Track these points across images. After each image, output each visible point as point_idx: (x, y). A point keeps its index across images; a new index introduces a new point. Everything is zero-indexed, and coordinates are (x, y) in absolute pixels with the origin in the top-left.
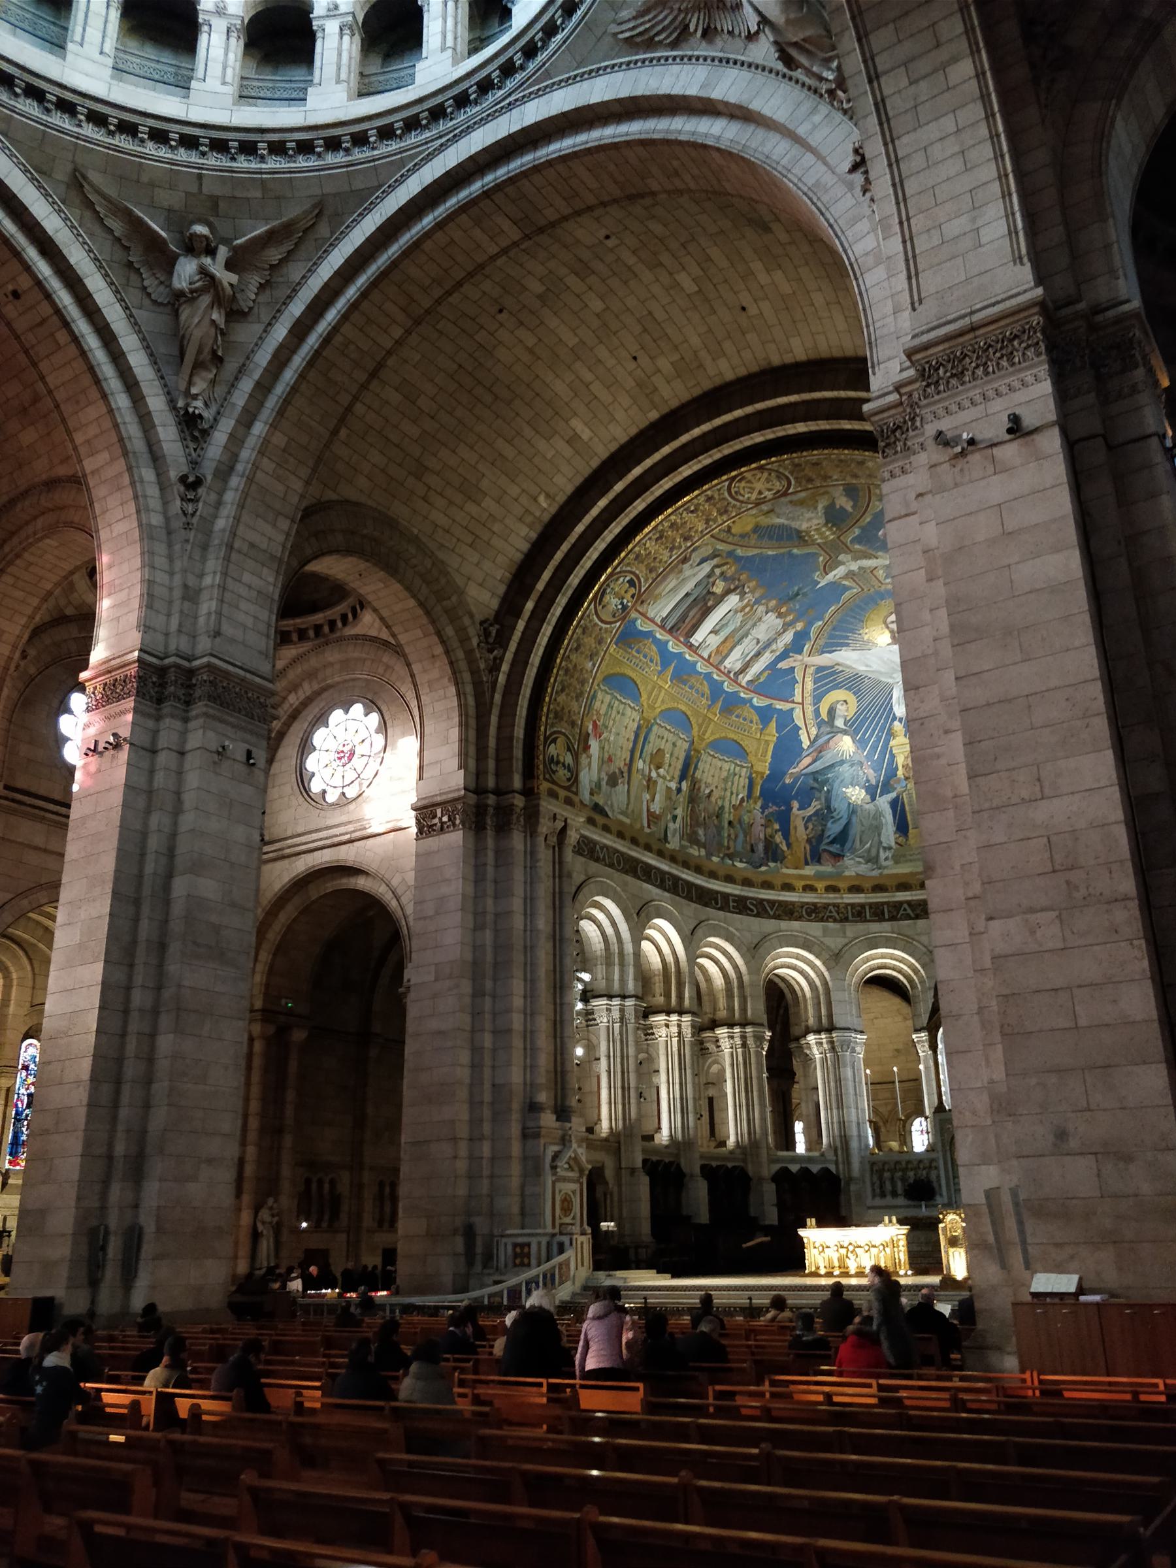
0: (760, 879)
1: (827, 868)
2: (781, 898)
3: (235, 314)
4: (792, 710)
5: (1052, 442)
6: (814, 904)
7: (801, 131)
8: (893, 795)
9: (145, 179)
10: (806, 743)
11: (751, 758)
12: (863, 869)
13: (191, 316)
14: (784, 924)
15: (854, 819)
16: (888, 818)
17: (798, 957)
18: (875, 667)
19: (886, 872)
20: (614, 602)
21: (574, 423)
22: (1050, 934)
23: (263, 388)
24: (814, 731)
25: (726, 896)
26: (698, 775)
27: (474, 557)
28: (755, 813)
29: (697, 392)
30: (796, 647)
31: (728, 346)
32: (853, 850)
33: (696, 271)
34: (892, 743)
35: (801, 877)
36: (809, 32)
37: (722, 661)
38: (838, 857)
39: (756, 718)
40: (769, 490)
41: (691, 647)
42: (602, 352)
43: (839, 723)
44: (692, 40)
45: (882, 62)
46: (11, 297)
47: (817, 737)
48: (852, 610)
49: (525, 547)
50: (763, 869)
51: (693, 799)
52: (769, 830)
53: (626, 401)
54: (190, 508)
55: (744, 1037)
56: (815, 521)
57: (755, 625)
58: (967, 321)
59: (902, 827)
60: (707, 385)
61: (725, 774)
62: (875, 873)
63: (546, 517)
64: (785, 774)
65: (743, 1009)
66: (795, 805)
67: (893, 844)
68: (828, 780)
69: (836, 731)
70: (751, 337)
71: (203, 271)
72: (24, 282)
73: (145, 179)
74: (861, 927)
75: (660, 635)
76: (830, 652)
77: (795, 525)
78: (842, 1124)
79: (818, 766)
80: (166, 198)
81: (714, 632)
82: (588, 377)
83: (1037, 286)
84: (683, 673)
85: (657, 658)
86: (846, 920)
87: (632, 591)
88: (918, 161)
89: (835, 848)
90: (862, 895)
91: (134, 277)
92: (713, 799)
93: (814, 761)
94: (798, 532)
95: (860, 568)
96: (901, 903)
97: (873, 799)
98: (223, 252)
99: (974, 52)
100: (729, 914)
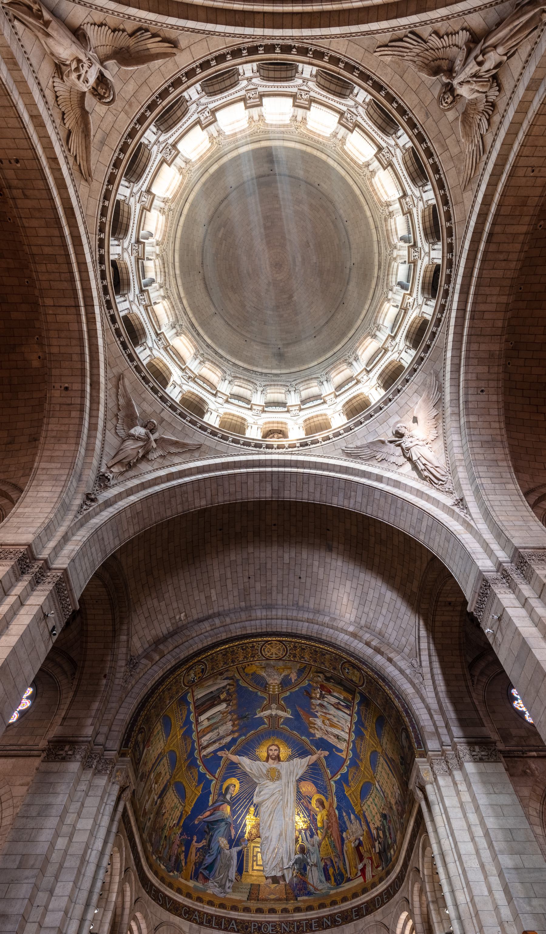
0: (168, 880)
1: (200, 885)
2: (175, 898)
4: (212, 780)
6: (189, 907)
8: (240, 848)
10: (210, 803)
11: (186, 801)
15: (219, 857)
16: (235, 862)
19: (228, 896)
20: (193, 675)
21: (213, 591)
25: (152, 885)
26: (165, 798)
28: (177, 836)
30: (227, 747)
31: (285, 590)
33: (293, 555)
34: (247, 817)
35: (187, 886)
37: (202, 737)
38: (206, 879)
39: (197, 778)
40: (276, 654)
41: (197, 721)
42: (239, 569)
43: (228, 797)
48: (259, 737)
49: (165, 632)
50: (171, 874)
52: (180, 850)
53: (236, 593)
56: (276, 681)
57: (222, 725)
60: (269, 602)
61: (173, 805)
62: (222, 895)
63: (180, 624)
64: (196, 817)
66: (195, 838)
67: (234, 879)
68: (213, 828)
69: (225, 801)
70: (296, 591)
76: (240, 756)
79: (211, 818)
81: (208, 719)
82: (229, 575)
85: (184, 718)
86: (201, 924)
87: (201, 675)
89: (206, 873)
90: (214, 908)
92: (164, 817)
93: (211, 815)
94: (267, 684)
95: (276, 715)
96: (232, 919)
97: (230, 848)
100: (150, 899)
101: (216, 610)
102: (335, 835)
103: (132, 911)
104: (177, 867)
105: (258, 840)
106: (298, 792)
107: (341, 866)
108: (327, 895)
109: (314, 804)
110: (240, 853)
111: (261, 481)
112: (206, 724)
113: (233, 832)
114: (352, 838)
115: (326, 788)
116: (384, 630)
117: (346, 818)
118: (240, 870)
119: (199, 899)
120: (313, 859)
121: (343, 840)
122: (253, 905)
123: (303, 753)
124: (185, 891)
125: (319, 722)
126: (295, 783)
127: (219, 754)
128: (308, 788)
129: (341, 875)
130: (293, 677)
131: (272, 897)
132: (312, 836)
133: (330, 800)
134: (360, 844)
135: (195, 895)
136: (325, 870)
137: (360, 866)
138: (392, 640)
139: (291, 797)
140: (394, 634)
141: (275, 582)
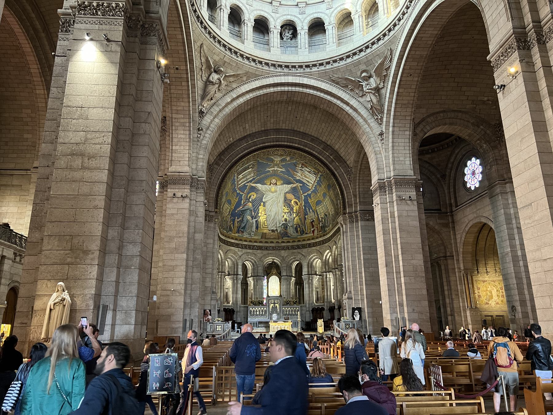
1: (240, 235)
5: (415, 203)
7: (369, 121)
9: (214, 52)
12: (247, 236)
13: (212, 88)
16: (255, 224)
17: (232, 256)
18: (263, 189)
21: (247, 125)
22: (413, 281)
23: (220, 111)
24: (245, 201)
29: (275, 128)
30: (251, 181)
31: (287, 122)
32: (246, 231)
36: (379, 108)
38: (243, 232)
41: (238, 178)
42: (262, 114)
43: (250, 200)
44: (347, 89)
45: (396, 125)
46: (175, 68)
47: (245, 202)
53: (259, 124)
54: (199, 136)
58: (403, 177)
59: (257, 228)
60: (278, 127)
63: (230, 143)
65: (222, 269)
66: (236, 218)
71: (219, 79)
72: (183, 67)
73: (214, 52)
74: (246, 250)
77: (274, 159)
78: (236, 298)
79: (243, 209)
80: (217, 58)
82: (256, 116)
83: (414, 176)
84: (233, 183)
86: (242, 248)
88: (397, 144)
89: (242, 230)
91: (201, 73)
99: (410, 131)
101: (248, 133)
102: (302, 216)
104: (231, 230)
105: (265, 216)
106: (285, 197)
108: (296, 238)
110: (256, 221)
111: (281, 94)
112: (242, 177)
113: (253, 213)
114: (310, 218)
115: (299, 197)
116: (339, 150)
119: (241, 240)
121: (305, 218)
122: (263, 240)
123: (289, 183)
124: (235, 238)
125: (299, 175)
126: (284, 194)
127: (246, 184)
128: (290, 196)
129: (303, 231)
130: (288, 159)
131: (272, 237)
133: (301, 202)
134: (313, 221)
135: (239, 239)
136: (296, 229)
137: (312, 229)
138: (342, 155)
139: (282, 199)
140: (344, 153)
141: (282, 118)
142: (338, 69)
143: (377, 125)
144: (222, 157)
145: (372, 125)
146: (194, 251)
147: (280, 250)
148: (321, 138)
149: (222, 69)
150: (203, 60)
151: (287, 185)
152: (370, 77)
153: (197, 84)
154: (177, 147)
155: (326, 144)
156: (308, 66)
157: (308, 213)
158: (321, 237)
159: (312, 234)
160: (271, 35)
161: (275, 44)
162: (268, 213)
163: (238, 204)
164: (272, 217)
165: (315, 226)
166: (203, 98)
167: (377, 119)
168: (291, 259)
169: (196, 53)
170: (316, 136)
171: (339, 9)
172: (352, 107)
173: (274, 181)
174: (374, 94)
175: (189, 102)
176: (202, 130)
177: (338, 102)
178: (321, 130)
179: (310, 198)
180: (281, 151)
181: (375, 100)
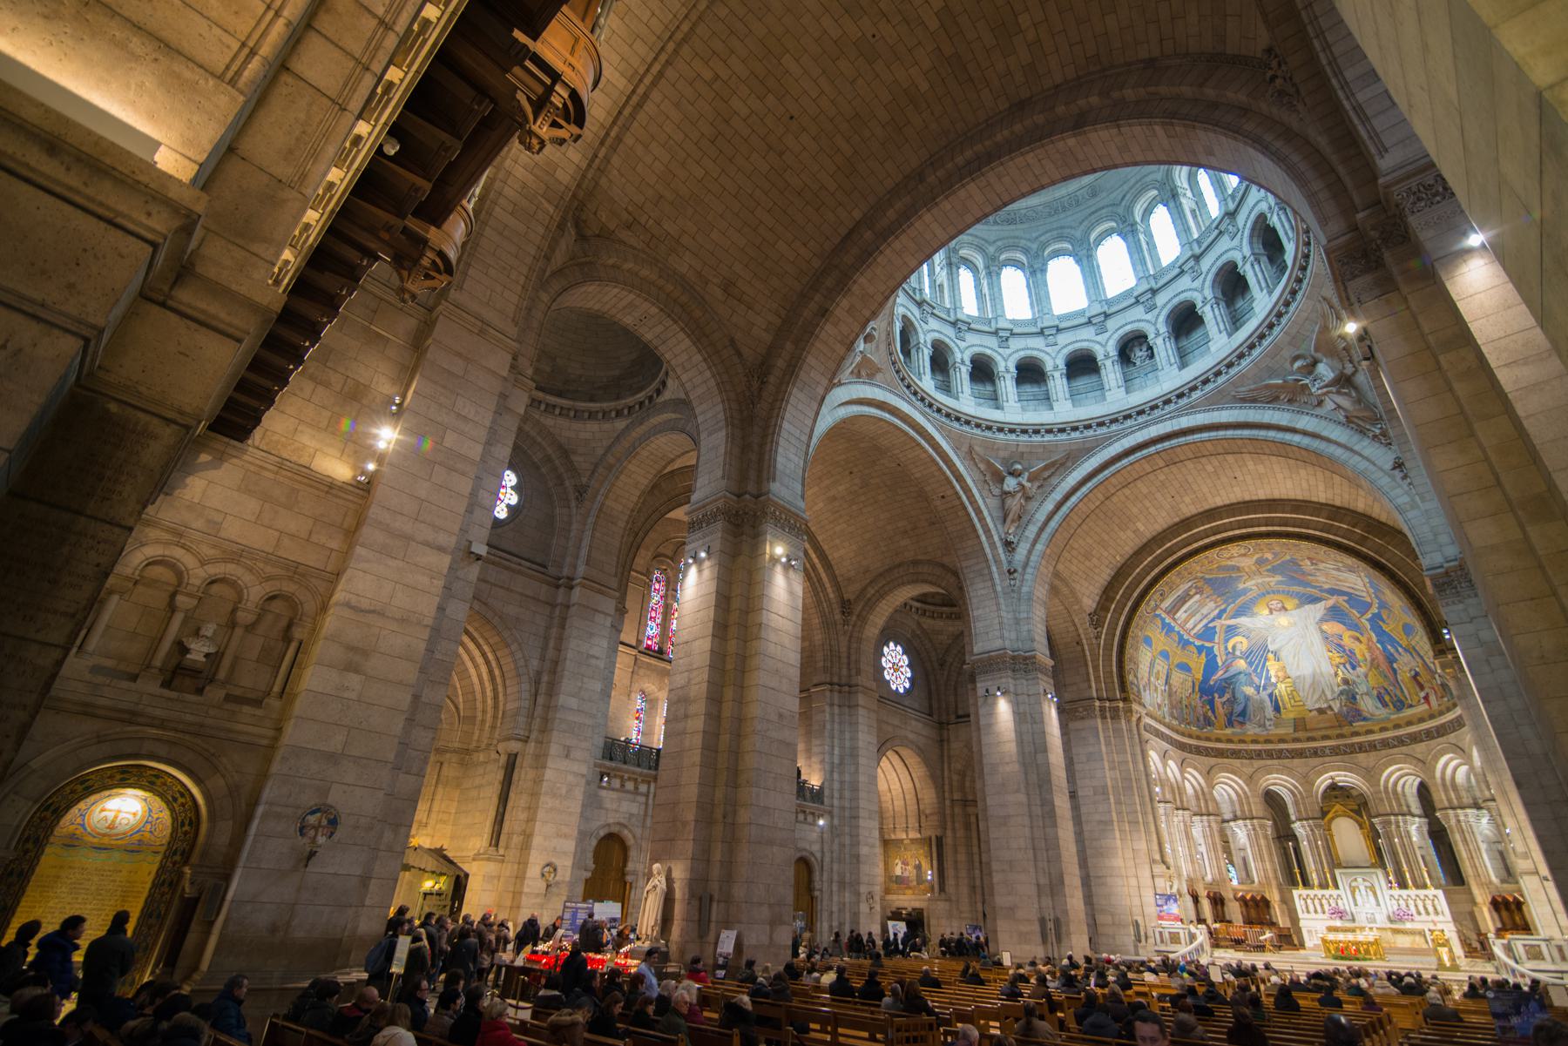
0: (1203, 736)
1: (1237, 730)
3: (1028, 498)
8: (1269, 691)
10: (1220, 664)
12: (1258, 730)
14: (1220, 760)
16: (1268, 703)
23: (1042, 529)
27: (1086, 584)
29: (1201, 510)
30: (1219, 616)
31: (1222, 492)
38: (1243, 724)
42: (1158, 495)
43: (1238, 653)
49: (1109, 579)
51: (1170, 695)
55: (1209, 822)
59: (1277, 709)
66: (1216, 695)
69: (1235, 657)
71: (1020, 484)
72: (949, 492)
74: (1262, 763)
75: (1164, 615)
79: (1226, 675)
80: (1002, 454)
82: (1148, 504)
84: (1168, 629)
89: (1240, 719)
98: (1026, 474)
102: (1384, 666)
103: (1182, 772)
104: (1208, 722)
106: (1322, 632)
107: (1398, 693)
109: (1347, 641)
110: (1271, 695)
112: (1185, 615)
114: (1406, 669)
117: (1392, 650)
118: (1277, 709)
120: (1362, 689)
121: (1395, 671)
122: (1300, 734)
123: (1314, 600)
124: (1224, 738)
125: (1322, 579)
128: (1333, 628)
129: (1401, 702)
132: (1354, 668)
134: (1417, 674)
136: (1380, 698)
137: (1422, 694)
139: (1316, 638)
141: (1205, 490)
142: (1242, 377)
143: (1383, 449)
144: (1111, 594)
145: (1366, 452)
146: (1040, 787)
147: (1352, 753)
148: (1314, 499)
149: (1019, 467)
150: (982, 466)
151: (1311, 606)
152: (1315, 363)
153: (986, 505)
154: (980, 612)
155: (1333, 506)
156: (1180, 396)
157: (1396, 655)
158: (1449, 710)
159: (1426, 707)
160: (1103, 372)
161: (1113, 384)
162: (1293, 673)
163: (1211, 666)
164: (1309, 681)
165: (1426, 685)
166: (1005, 521)
167: (1375, 436)
168: (1392, 773)
169: (966, 463)
170: (1300, 498)
171: (1214, 270)
172: (1305, 433)
173: (1275, 604)
174: (1338, 393)
175: (978, 537)
176: (1015, 571)
177: (1272, 434)
178: (1305, 485)
179: (1383, 620)
180: (1234, 549)
181: (1345, 402)
